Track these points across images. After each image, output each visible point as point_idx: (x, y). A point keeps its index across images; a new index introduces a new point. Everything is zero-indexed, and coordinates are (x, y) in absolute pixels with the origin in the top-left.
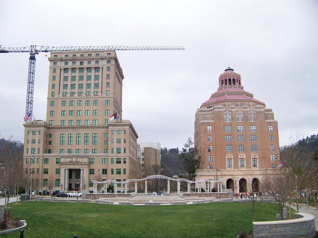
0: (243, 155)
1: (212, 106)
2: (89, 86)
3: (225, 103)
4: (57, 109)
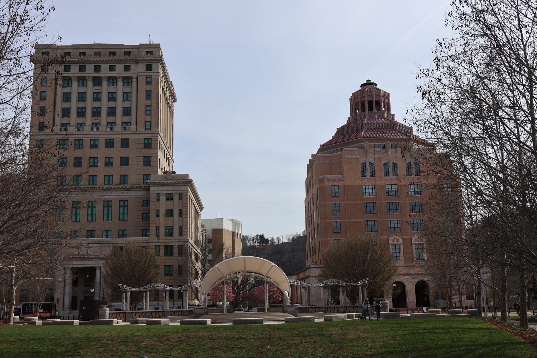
0: (398, 237)
2: (112, 112)
3: (362, 144)
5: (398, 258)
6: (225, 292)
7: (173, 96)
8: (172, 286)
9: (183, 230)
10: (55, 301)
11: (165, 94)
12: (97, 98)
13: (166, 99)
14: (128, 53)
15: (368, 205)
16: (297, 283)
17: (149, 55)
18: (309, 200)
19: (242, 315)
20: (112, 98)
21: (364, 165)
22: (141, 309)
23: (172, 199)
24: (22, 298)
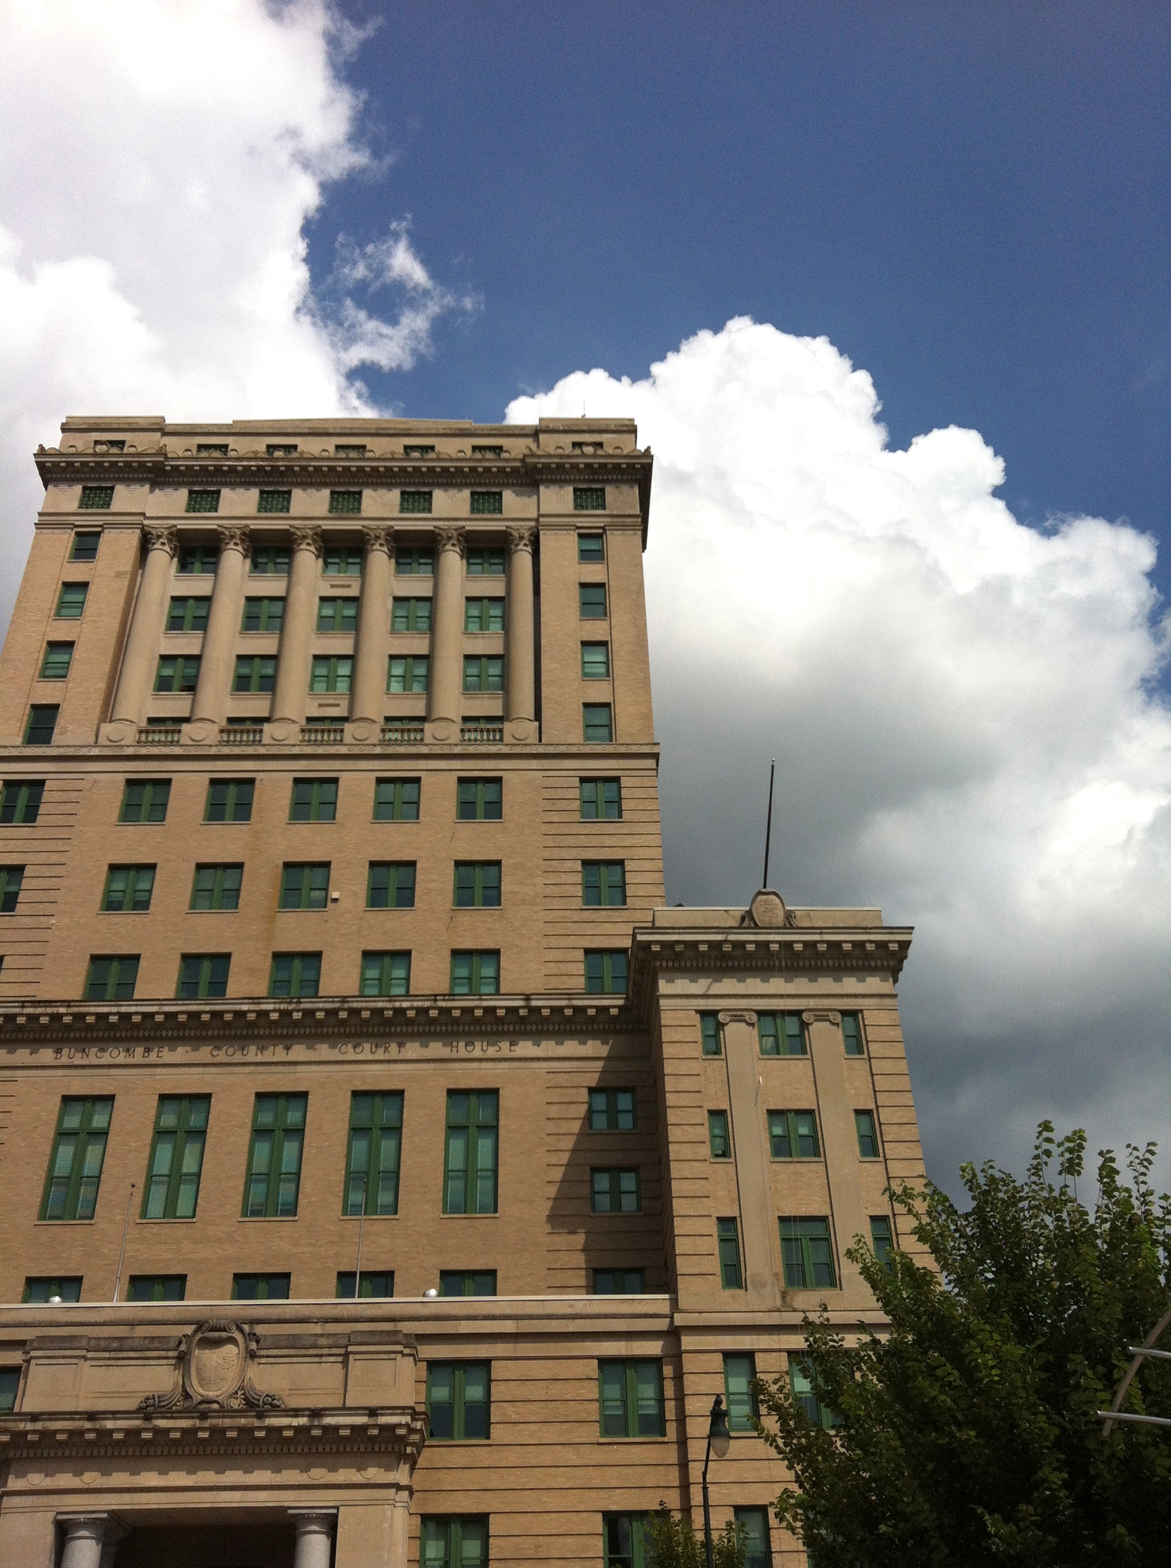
4: (60, 845)
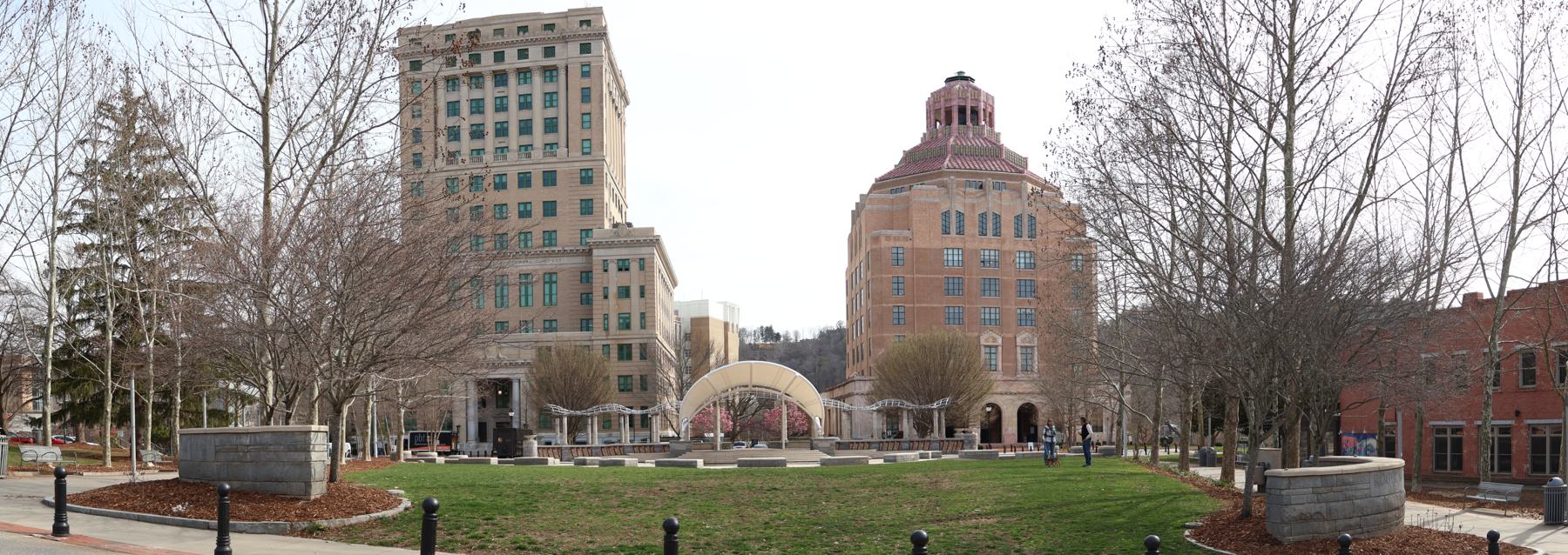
0: (994, 335)
1: (907, 186)
2: (526, 128)
5: (993, 368)
6: (719, 417)
7: (623, 95)
8: (631, 408)
9: (646, 319)
10: (455, 429)
11: (611, 93)
12: (501, 106)
13: (613, 101)
14: (550, 27)
15: (951, 281)
16: (832, 404)
17: (585, 27)
18: (853, 270)
19: (745, 452)
20: (525, 104)
21: (946, 215)
22: (585, 443)
23: (627, 269)
24: (410, 425)
